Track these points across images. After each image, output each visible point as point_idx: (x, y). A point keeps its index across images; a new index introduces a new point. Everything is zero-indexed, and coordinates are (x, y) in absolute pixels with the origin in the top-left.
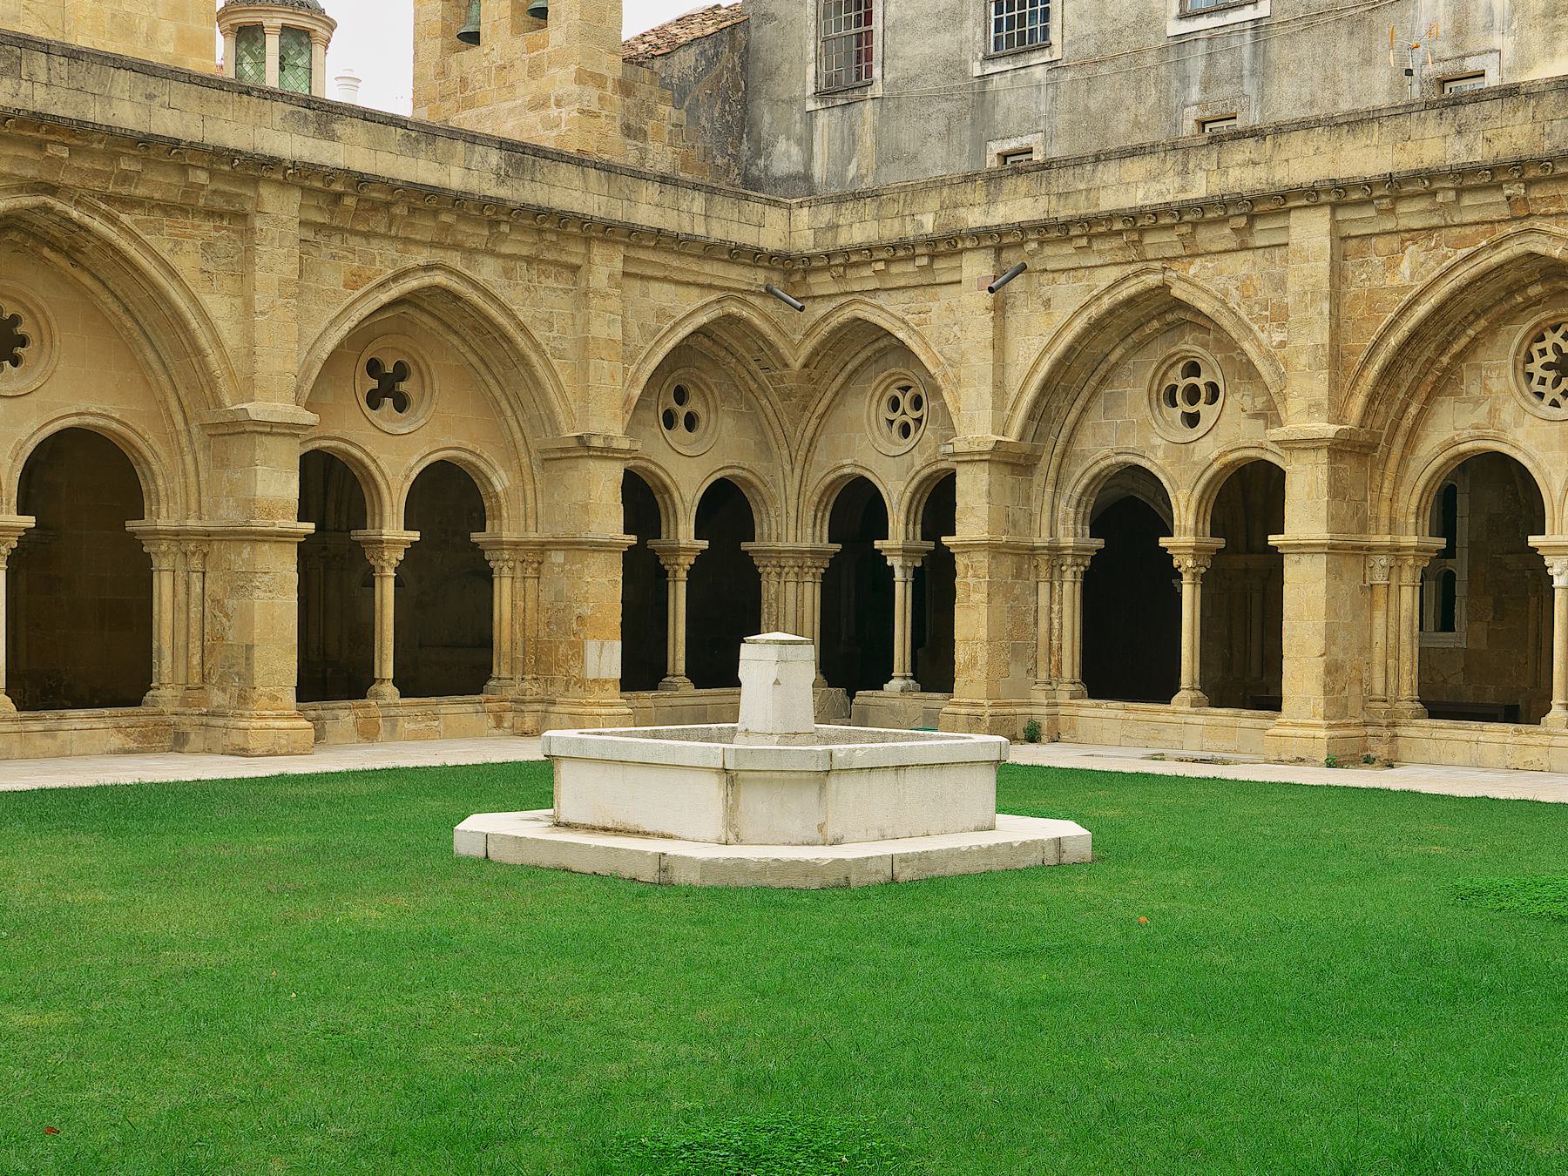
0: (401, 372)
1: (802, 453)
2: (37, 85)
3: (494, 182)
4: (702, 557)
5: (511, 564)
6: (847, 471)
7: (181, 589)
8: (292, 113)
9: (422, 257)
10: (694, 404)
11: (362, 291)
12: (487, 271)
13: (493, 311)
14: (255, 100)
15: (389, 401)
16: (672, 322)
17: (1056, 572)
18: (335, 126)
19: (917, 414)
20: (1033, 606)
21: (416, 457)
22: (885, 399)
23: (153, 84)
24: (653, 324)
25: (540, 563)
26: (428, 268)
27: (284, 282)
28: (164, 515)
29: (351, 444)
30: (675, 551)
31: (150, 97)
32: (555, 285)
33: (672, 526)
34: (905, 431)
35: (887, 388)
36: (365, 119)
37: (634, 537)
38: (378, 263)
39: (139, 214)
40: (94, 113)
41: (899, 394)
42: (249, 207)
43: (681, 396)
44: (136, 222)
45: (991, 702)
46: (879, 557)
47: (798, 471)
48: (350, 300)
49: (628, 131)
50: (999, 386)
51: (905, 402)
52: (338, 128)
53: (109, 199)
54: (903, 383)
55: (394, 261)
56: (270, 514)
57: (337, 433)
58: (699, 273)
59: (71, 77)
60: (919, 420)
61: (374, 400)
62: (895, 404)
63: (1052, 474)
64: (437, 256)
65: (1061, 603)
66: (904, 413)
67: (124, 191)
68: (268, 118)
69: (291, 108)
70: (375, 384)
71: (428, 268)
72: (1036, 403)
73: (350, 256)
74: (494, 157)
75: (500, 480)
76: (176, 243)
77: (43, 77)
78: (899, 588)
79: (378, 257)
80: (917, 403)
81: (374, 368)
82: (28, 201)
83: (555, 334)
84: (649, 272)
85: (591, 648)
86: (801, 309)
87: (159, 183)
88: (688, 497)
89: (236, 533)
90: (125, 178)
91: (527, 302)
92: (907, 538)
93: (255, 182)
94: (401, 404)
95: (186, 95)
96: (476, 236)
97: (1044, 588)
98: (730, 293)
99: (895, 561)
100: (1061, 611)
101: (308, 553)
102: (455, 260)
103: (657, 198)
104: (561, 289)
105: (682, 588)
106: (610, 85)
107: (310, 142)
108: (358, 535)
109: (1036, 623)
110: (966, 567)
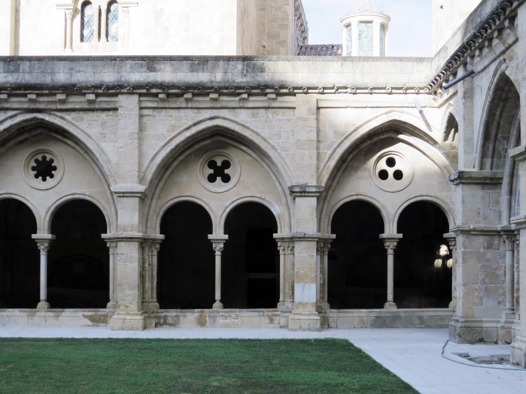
0: (227, 164)
2: (26, 74)
3: (240, 76)
8: (135, 64)
12: (243, 116)
14: (118, 62)
18: (156, 66)
23: (73, 65)
26: (211, 119)
27: (132, 134)
29: (196, 198)
31: (71, 69)
32: (282, 118)
36: (171, 60)
37: (335, 235)
38: (184, 120)
39: (74, 114)
40: (48, 80)
42: (117, 105)
44: (73, 118)
45: (464, 320)
52: (158, 66)
55: (193, 119)
56: (124, 230)
57: (189, 194)
59: (39, 68)
61: (212, 179)
67: (64, 107)
68: (123, 69)
69: (135, 62)
70: (212, 171)
71: (211, 119)
73: (170, 119)
74: (240, 66)
75: (276, 210)
76: (89, 124)
77: (28, 70)
79: (184, 117)
81: (212, 164)
83: (282, 140)
87: (76, 101)
91: (266, 127)
93: (116, 95)
94: (226, 179)
95: (87, 65)
96: (233, 101)
104: (286, 120)
107: (144, 74)
109: (505, 275)
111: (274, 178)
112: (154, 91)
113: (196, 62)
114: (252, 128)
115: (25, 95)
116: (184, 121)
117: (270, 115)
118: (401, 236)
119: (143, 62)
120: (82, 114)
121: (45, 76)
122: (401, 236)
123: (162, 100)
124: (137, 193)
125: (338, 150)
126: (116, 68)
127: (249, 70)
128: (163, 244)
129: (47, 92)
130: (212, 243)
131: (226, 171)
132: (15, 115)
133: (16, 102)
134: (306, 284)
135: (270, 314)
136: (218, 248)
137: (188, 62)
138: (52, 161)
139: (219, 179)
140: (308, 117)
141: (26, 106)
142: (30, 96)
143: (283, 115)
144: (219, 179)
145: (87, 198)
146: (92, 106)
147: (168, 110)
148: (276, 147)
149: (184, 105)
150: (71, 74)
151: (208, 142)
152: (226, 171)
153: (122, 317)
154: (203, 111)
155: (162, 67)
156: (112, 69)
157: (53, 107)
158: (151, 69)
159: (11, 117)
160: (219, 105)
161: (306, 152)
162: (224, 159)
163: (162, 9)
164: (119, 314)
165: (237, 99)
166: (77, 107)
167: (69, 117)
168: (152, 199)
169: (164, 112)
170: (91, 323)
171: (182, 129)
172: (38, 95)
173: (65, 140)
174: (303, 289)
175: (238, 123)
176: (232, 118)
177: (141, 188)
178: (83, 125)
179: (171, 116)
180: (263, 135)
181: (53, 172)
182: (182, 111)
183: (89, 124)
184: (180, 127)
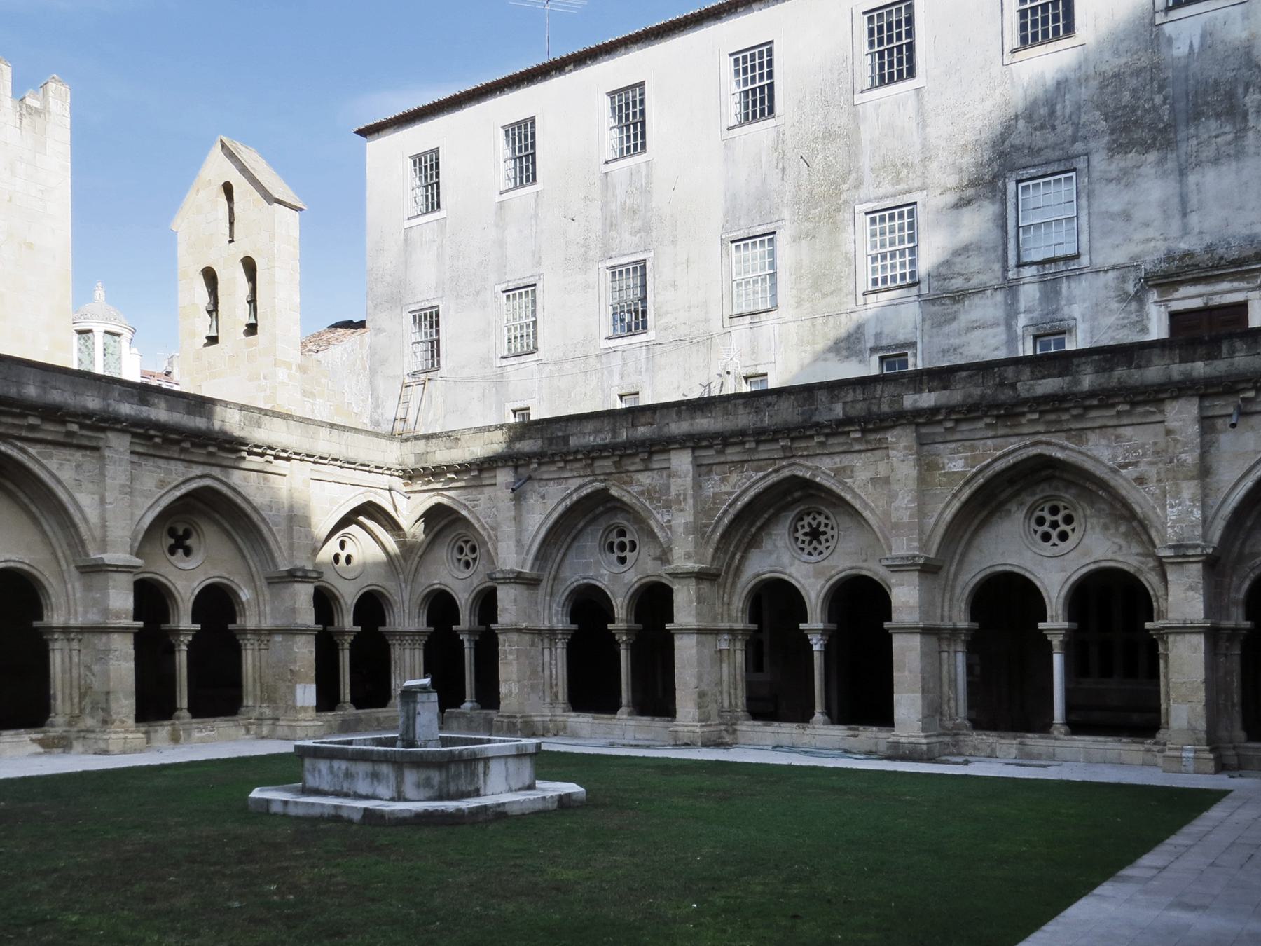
1: (411, 577)
5: (252, 641)
6: (436, 587)
7: (67, 660)
9: (198, 471)
11: (166, 490)
13: (239, 501)
15: (180, 551)
16: (338, 506)
17: (553, 643)
19: (474, 556)
20: (541, 662)
21: (196, 584)
22: (457, 546)
25: (268, 641)
27: (123, 486)
28: (56, 617)
33: (340, 619)
34: (467, 565)
35: (457, 541)
41: (463, 544)
42: (101, 444)
44: (38, 453)
46: (456, 635)
47: (409, 587)
48: (159, 495)
49: (305, 393)
50: (518, 541)
51: (467, 549)
54: (465, 539)
60: (475, 560)
62: (461, 550)
63: (549, 590)
64: (207, 470)
65: (556, 660)
66: (466, 555)
67: (31, 435)
72: (539, 550)
73: (159, 471)
76: (61, 465)
78: (467, 651)
80: (473, 549)
83: (273, 512)
85: (299, 689)
86: (409, 498)
87: (52, 430)
88: (349, 602)
89: (99, 628)
90: (32, 428)
92: (471, 624)
97: (547, 652)
99: (464, 637)
100: (556, 664)
102: (216, 472)
105: (347, 653)
106: (294, 368)
107: (135, 407)
108: (164, 627)
109: (543, 671)
110: (505, 641)
112: (152, 432)
113: (193, 402)
119: (134, 391)
120: (50, 449)
121: (8, 386)
123: (156, 446)
127: (247, 423)
137: (185, 400)
146: (69, 440)
147: (156, 459)
149: (176, 456)
153: (122, 736)
154: (194, 466)
155: (156, 401)
157: (15, 432)
158: (144, 402)
160: (213, 461)
162: (187, 526)
165: (177, 448)
166: (50, 437)
167: (33, 450)
169: (150, 462)
170: (41, 750)
178: (52, 465)
179: (159, 467)
182: (172, 463)
183: (61, 465)
184: (169, 483)
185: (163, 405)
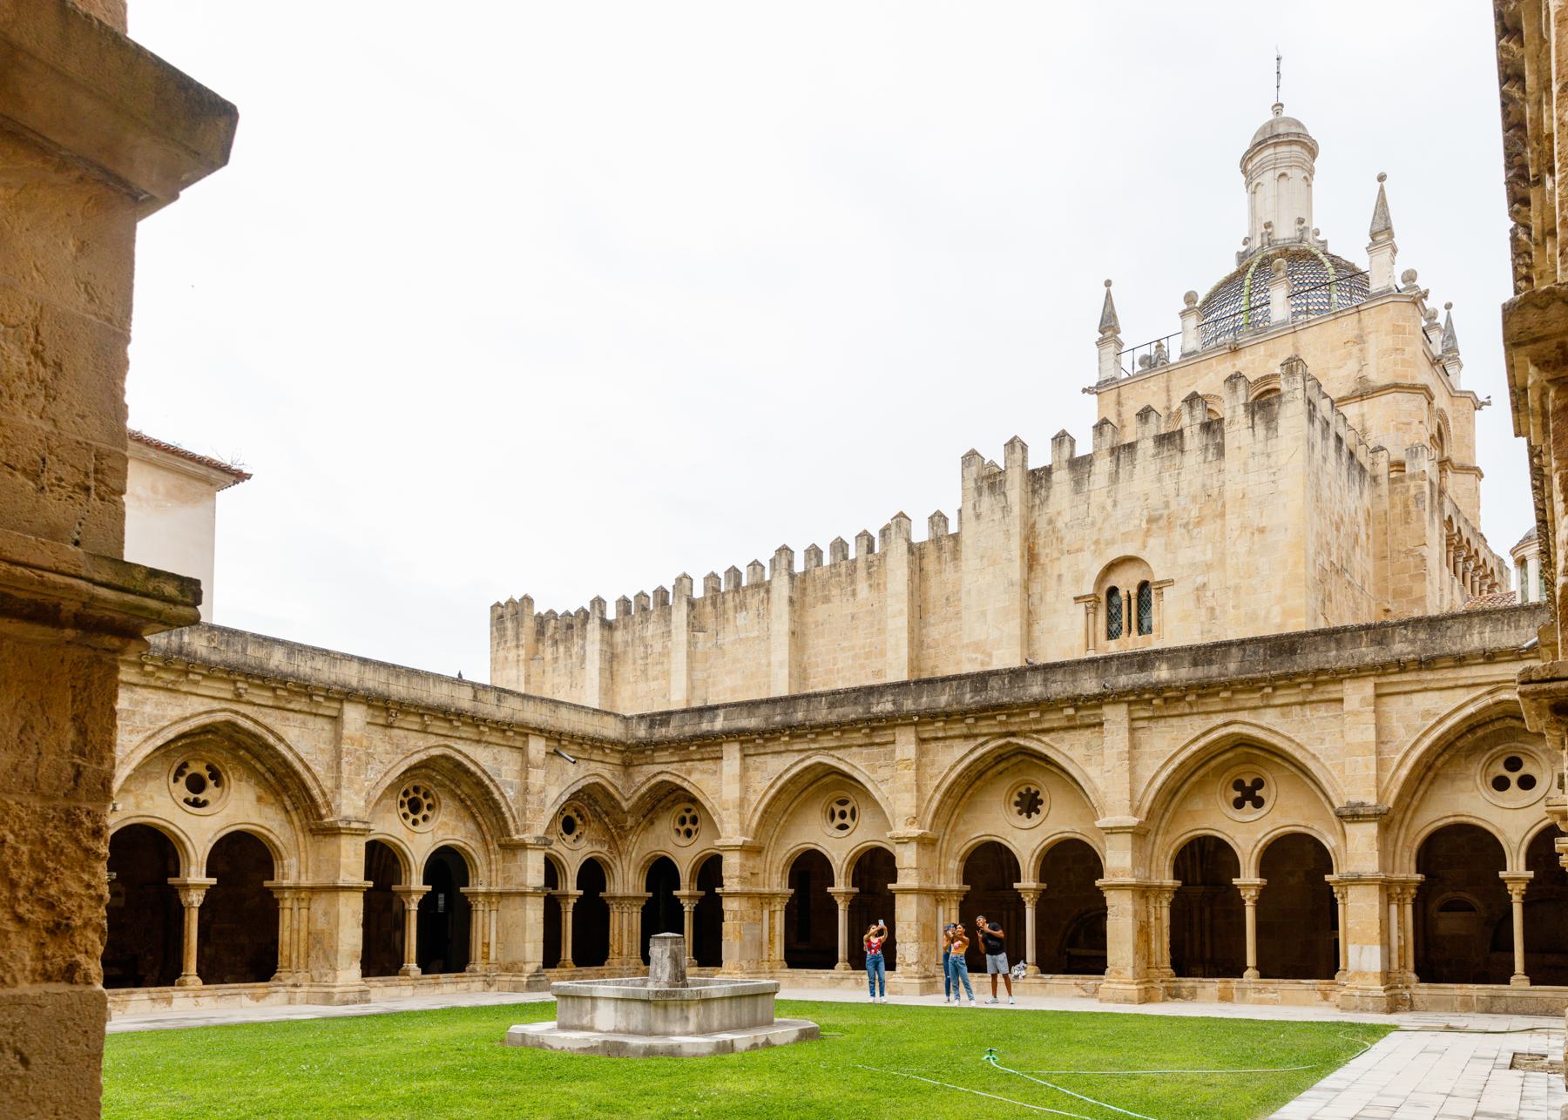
4: (211, 892)
9: (1219, 719)
10: (1527, 768)
24: (1418, 722)
26: (1226, 725)
30: (409, 893)
39: (1053, 735)
43: (1513, 764)
44: (1052, 740)
53: (1037, 732)
58: (1457, 679)
67: (1039, 727)
71: (1226, 725)
76: (1071, 745)
82: (1002, 742)
83: (1327, 746)
84: (1407, 688)
87: (1053, 719)
90: (1037, 721)
93: (1099, 706)
98: (1498, 686)
101: (368, 896)
103: (1410, 635)
107: (1133, 676)
111: (1323, 799)
114: (1281, 732)
115: (994, 717)
116: (1190, 731)
117: (1308, 713)
118: (1531, 874)
120: (1062, 734)
122: (1531, 874)
123: (1159, 707)
124: (1129, 827)
125: (1413, 752)
126: (1099, 672)
128: (1177, 893)
129: (1018, 711)
130: (1239, 890)
131: (1258, 793)
132: (986, 742)
133: (984, 727)
134: (1366, 947)
135: (1323, 987)
136: (1249, 898)
138: (1037, 793)
139: (1248, 803)
140: (1361, 709)
141: (997, 730)
142: (998, 718)
143: (1326, 711)
144: (1248, 803)
145: (1078, 836)
146: (1073, 723)
147: (1168, 719)
148: (1318, 755)
149: (1187, 711)
150: (1046, 686)
151: (1229, 755)
152: (1258, 793)
154: (1213, 716)
156: (1093, 675)
157: (1026, 728)
159: (982, 745)
160: (1234, 706)
161: (1359, 759)
162: (1255, 776)
163: (1205, 584)
164: (1108, 982)
167: (1045, 739)
168: (1156, 834)
169: (1162, 722)
171: (1187, 741)
172: (1009, 716)
173: (1048, 766)
174: (1361, 953)
175: (1262, 728)
176: (1254, 721)
177: (1133, 821)
178: (1064, 748)
180: (1298, 741)
181: (1039, 807)
182: (1186, 719)
183: (1071, 745)
185: (1164, 666)
